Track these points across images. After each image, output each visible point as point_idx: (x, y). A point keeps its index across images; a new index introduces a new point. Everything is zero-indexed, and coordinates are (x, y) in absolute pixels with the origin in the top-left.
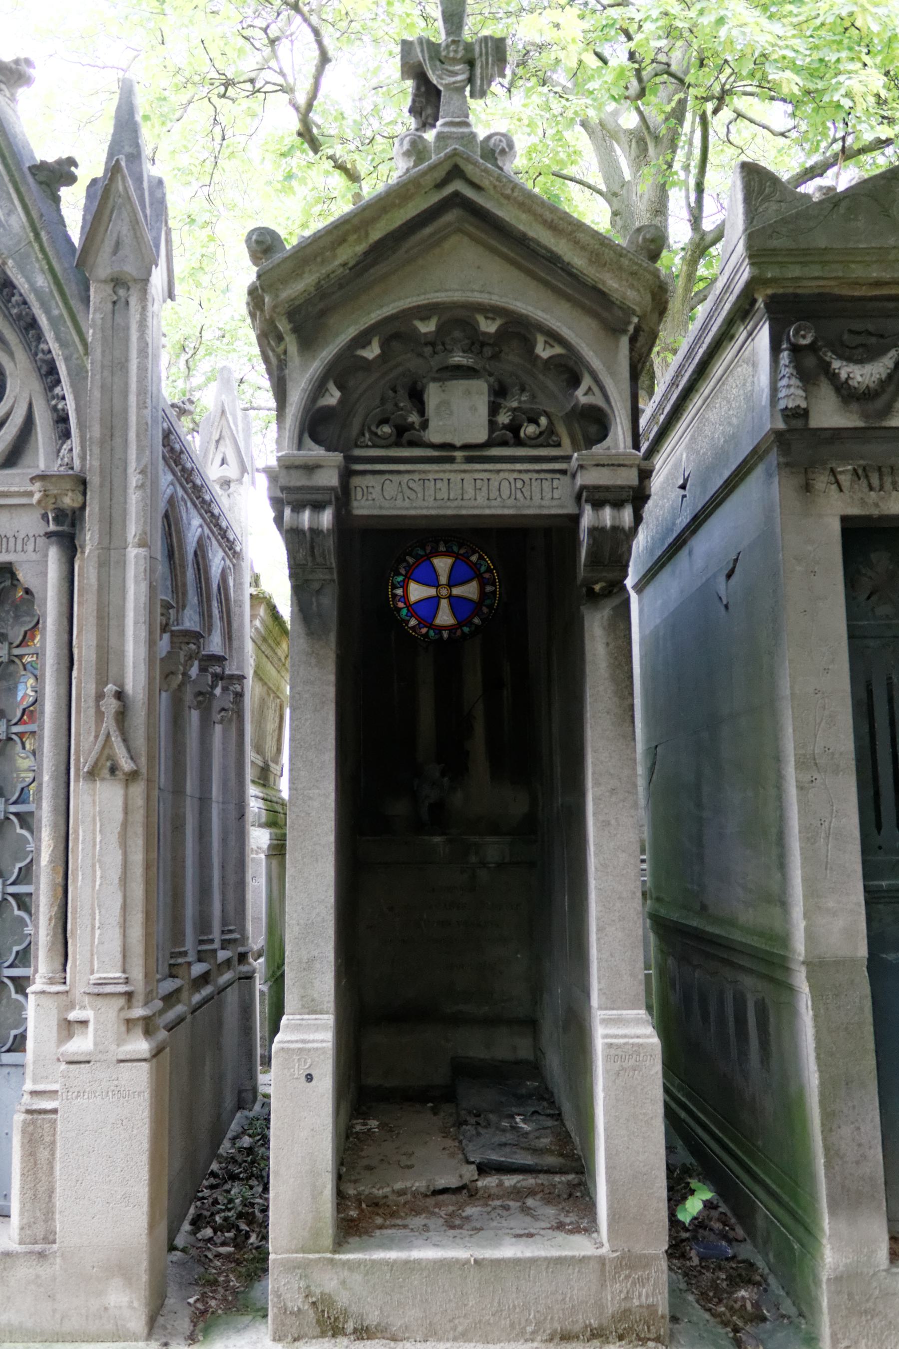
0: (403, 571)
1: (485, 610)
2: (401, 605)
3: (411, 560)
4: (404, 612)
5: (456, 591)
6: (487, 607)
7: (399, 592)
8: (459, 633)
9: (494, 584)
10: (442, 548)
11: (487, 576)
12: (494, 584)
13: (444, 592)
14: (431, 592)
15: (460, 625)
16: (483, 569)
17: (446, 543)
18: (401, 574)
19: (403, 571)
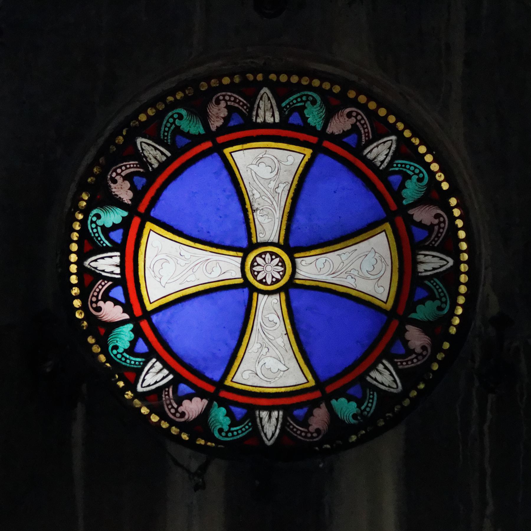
0: (123, 191)
1: (416, 338)
2: (111, 312)
3: (153, 153)
4: (124, 336)
5: (313, 268)
6: (424, 326)
7: (108, 264)
8: (319, 418)
9: (449, 246)
10: (266, 113)
11: (424, 215)
12: (449, 246)
13: (269, 270)
14: (225, 267)
15: (323, 390)
16: (412, 191)
17: (280, 93)
18: (119, 203)
19: (123, 191)
